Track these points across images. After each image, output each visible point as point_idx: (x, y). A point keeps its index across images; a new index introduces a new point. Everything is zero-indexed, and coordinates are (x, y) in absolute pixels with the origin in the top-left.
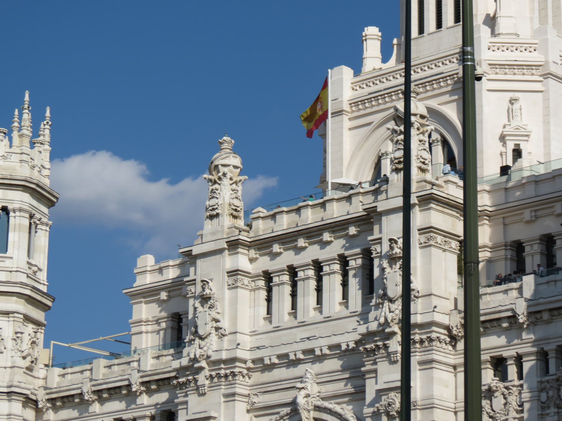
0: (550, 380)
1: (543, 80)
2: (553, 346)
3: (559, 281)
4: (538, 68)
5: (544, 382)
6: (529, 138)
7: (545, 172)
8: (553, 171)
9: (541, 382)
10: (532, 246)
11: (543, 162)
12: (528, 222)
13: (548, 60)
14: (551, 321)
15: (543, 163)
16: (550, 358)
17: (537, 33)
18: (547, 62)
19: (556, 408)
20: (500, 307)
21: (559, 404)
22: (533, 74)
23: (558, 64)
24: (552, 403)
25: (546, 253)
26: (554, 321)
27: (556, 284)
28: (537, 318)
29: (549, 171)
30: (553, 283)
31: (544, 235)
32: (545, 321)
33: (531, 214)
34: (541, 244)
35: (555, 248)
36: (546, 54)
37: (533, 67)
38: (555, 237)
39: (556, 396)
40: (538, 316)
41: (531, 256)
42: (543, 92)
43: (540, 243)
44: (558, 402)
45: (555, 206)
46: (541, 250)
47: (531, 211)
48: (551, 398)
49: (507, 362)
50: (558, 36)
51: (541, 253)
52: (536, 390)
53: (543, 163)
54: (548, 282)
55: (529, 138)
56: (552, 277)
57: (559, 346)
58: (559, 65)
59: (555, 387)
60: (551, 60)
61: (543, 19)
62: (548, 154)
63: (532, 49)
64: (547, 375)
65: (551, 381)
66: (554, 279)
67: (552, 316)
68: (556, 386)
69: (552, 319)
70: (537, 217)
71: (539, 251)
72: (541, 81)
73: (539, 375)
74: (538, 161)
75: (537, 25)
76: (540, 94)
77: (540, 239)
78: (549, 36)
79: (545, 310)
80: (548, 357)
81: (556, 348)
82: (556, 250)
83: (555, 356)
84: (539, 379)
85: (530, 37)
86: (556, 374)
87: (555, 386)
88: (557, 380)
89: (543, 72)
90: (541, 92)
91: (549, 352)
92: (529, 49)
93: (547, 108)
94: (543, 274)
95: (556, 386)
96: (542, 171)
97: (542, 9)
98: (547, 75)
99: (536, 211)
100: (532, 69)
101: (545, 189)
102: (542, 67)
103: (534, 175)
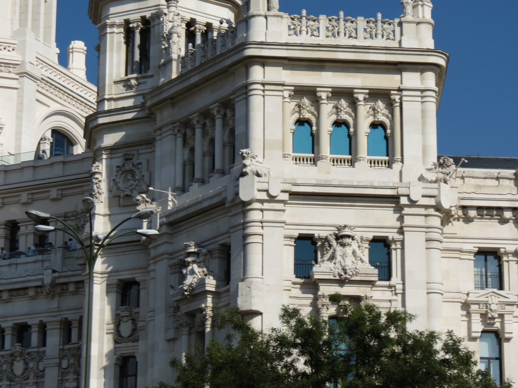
0: (5, 355)
1: (19, 78)
2: (10, 324)
3: (20, 264)
4: (15, 66)
5: (66, 350)
6: (2, 130)
7: (15, 163)
8: (22, 162)
9: (63, 350)
10: (27, 227)
11: (13, 154)
12: (54, 200)
13: (25, 60)
14: (10, 300)
15: (13, 155)
16: (73, 327)
17: (16, 34)
18: (23, 62)
19: (8, 381)
20: (69, 272)
21: (11, 377)
22: (10, 72)
23: (34, 65)
24: (5, 377)
25: (10, 238)
26: (39, 298)
27: (17, 267)
28: (38, 293)
29: (19, 162)
30: (14, 266)
31: (10, 221)
32: (4, 300)
33: (57, 192)
34: (6, 230)
35: (18, 233)
36: (23, 54)
37: (11, 66)
38: (49, 219)
39: (9, 370)
40: (64, 287)
41: (25, 236)
42: (18, 89)
43: (5, 228)
44: (10, 375)
45: (21, 195)
46: (6, 235)
47: (28, 194)
48: (5, 372)
49: (31, 329)
50: (35, 38)
51: (6, 238)
52: (58, 357)
53: (13, 155)
54: (9, 265)
55: (2, 130)
56: (13, 260)
57: (15, 324)
58: (35, 66)
59: (9, 362)
60: (27, 60)
61: (23, 22)
62: (18, 146)
63: (11, 49)
64: (3, 350)
65: (6, 356)
66: (15, 262)
67: (38, 293)
68: (10, 361)
69: (11, 299)
70: (63, 196)
71: (4, 235)
72: (17, 79)
73: (61, 343)
74: (9, 153)
75: (17, 27)
76: (16, 91)
77: (6, 225)
78: (27, 38)
79: (72, 282)
80: (4, 334)
81: (13, 326)
82: (19, 235)
83: (11, 333)
84: (61, 347)
85: (9, 38)
86: (10, 350)
87: (9, 360)
88: (12, 355)
89: (19, 71)
90: (16, 89)
91: (6, 329)
92: (8, 48)
93: (20, 104)
94: (6, 257)
95: (10, 361)
96: (12, 163)
97: (23, 13)
98: (23, 74)
99: (62, 190)
100: (10, 67)
101: (13, 178)
102: (19, 66)
103: (4, 165)
